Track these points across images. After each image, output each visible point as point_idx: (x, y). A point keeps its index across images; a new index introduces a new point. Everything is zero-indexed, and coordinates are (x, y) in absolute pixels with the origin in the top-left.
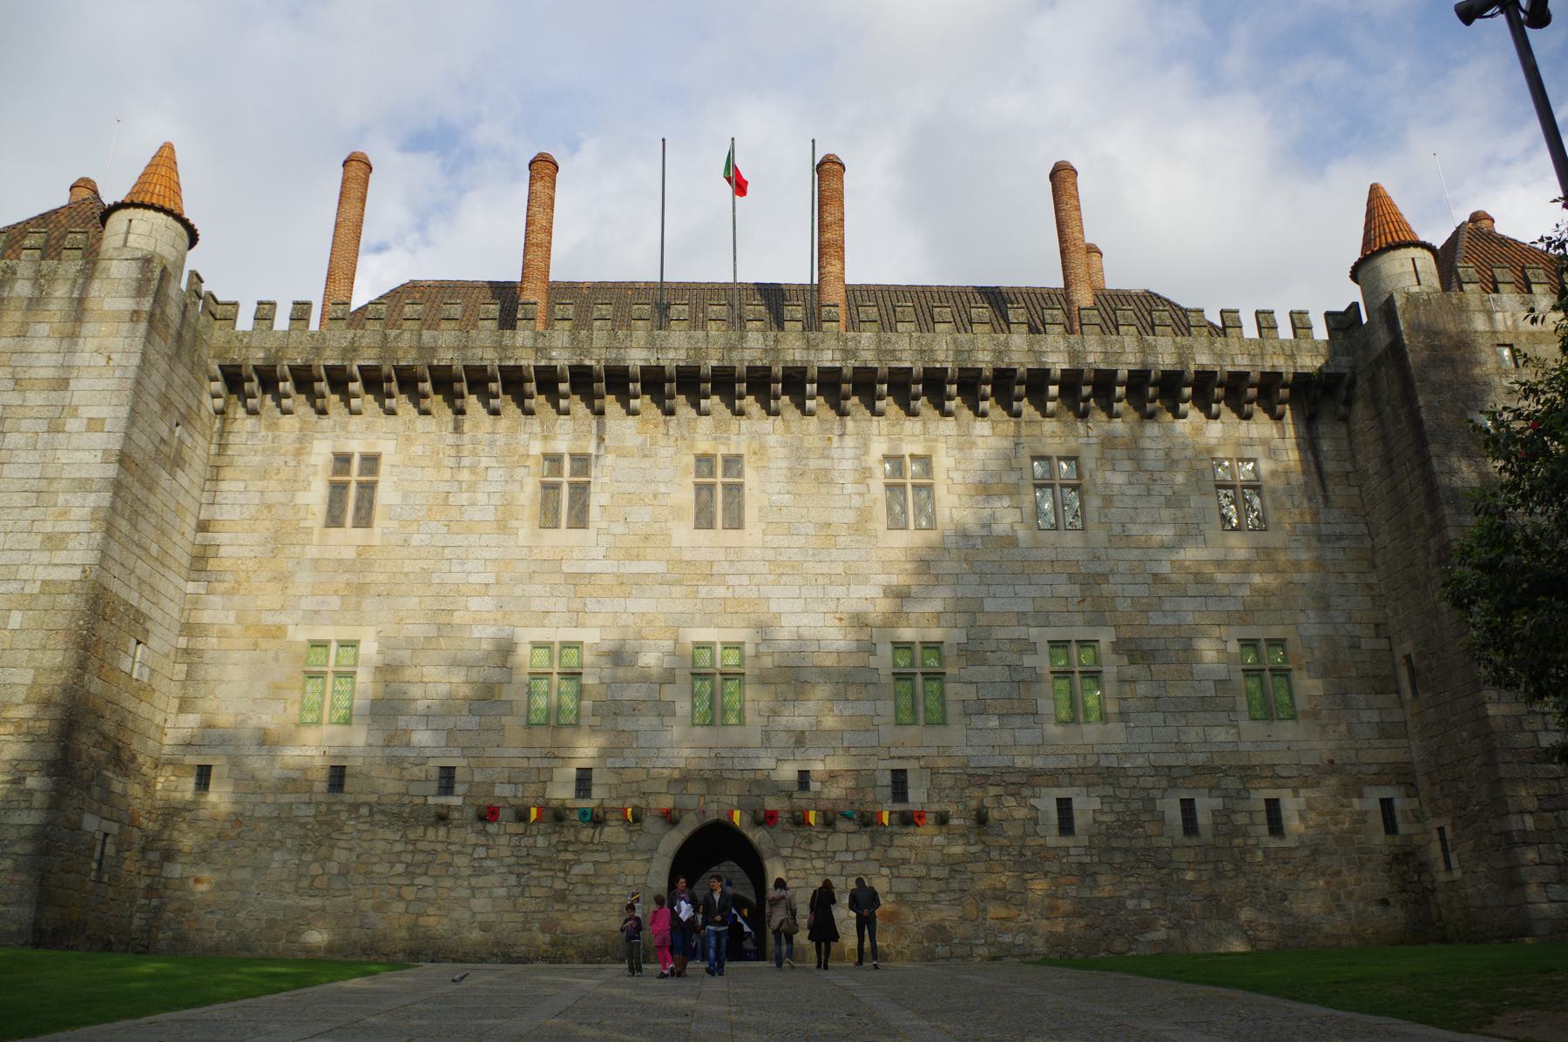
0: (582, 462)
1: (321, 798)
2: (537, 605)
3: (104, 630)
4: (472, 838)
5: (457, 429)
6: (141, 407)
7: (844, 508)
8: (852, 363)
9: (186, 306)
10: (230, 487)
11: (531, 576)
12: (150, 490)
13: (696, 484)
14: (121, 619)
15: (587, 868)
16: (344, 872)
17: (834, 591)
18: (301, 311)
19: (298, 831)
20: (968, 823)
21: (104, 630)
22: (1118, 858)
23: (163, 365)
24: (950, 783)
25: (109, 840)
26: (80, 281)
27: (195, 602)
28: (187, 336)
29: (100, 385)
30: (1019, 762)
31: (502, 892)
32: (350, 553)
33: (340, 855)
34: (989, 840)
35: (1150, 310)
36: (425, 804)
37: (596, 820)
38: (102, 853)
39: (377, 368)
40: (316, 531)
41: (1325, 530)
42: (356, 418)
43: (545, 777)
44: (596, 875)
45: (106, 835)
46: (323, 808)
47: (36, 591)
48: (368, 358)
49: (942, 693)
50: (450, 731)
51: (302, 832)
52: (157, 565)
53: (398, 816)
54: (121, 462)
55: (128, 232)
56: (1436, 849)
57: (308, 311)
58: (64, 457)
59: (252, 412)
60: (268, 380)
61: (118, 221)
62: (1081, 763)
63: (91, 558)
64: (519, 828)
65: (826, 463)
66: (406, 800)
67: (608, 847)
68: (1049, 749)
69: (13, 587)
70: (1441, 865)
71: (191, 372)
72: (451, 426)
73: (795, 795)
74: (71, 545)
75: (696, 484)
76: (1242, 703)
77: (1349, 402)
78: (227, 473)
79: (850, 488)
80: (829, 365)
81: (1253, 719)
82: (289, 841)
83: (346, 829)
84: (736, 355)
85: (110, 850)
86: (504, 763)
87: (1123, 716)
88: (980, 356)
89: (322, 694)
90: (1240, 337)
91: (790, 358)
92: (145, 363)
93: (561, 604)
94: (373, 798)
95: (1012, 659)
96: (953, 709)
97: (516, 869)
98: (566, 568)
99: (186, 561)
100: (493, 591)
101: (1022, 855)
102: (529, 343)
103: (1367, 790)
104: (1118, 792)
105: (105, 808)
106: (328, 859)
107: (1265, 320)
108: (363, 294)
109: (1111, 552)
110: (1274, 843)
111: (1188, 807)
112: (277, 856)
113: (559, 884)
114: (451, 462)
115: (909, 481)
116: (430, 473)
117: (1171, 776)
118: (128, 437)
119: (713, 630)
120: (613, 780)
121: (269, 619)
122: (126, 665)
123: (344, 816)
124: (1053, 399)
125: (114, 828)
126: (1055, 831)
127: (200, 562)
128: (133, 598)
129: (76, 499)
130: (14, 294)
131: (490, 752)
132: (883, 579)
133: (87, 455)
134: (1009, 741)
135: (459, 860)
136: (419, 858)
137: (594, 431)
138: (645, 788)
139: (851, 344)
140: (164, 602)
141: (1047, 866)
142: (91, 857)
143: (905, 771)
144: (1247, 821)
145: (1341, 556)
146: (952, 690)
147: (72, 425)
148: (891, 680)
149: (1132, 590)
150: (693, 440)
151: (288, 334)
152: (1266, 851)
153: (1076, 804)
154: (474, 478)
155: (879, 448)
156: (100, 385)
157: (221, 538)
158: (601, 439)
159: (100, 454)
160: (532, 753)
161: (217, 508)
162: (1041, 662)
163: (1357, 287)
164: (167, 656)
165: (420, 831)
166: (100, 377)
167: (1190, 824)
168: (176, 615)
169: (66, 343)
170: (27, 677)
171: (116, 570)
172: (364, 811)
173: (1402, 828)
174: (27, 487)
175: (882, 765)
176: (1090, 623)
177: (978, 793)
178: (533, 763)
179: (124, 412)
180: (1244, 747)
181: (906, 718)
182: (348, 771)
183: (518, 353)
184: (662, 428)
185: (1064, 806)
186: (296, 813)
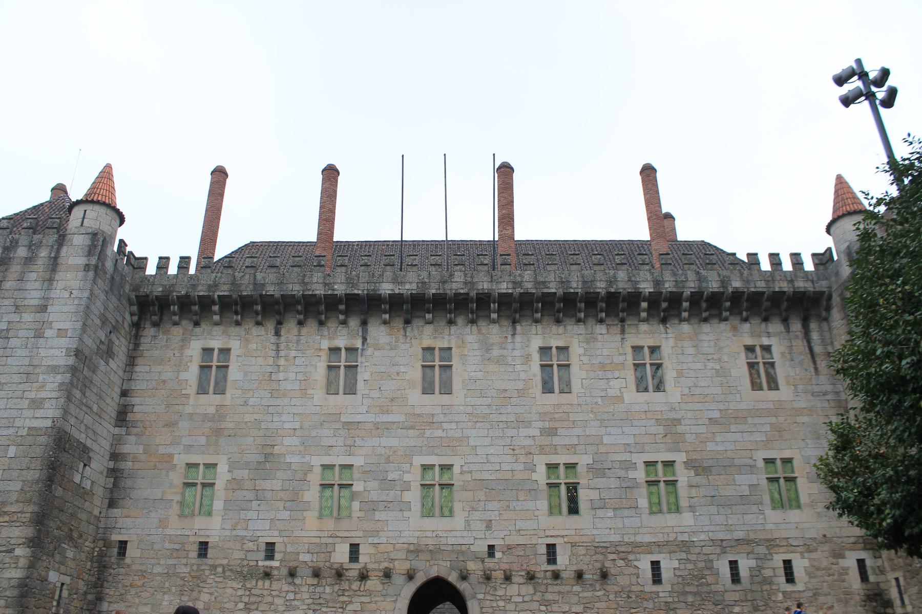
1: (193, 561)
2: (325, 442)
3: (64, 458)
4: (286, 587)
5: (277, 333)
6: (89, 322)
7: (515, 380)
8: (519, 290)
9: (117, 261)
11: (321, 424)
12: (94, 372)
13: (423, 366)
14: (75, 451)
17: (510, 432)
18: (184, 262)
21: (64, 458)
22: (690, 599)
23: (103, 296)
24: (583, 552)
25: (65, 587)
26: (56, 247)
27: (117, 440)
28: (117, 279)
29: (65, 309)
34: (608, 588)
35: (706, 254)
36: (257, 566)
38: (60, 596)
39: (229, 297)
40: (192, 397)
41: (816, 389)
42: (217, 328)
43: (328, 549)
45: (63, 584)
46: (195, 567)
47: (24, 434)
48: (224, 291)
51: (182, 582)
52: (97, 418)
53: (241, 572)
54: (75, 355)
55: (84, 218)
57: (188, 263)
58: (43, 352)
61: (77, 212)
62: (666, 538)
63: (58, 413)
64: (315, 581)
65: (505, 352)
66: (245, 563)
67: (370, 593)
68: (645, 530)
69: (11, 431)
71: (119, 300)
72: (273, 331)
73: (486, 560)
75: (423, 366)
76: (767, 499)
77: (828, 309)
78: (139, 361)
79: (519, 368)
80: (505, 291)
81: (774, 508)
82: (174, 588)
83: (209, 581)
84: (447, 286)
85: (65, 593)
87: (692, 508)
88: (598, 284)
89: (195, 496)
90: (759, 270)
91: (480, 287)
92: (92, 296)
93: (340, 442)
94: (225, 562)
95: (622, 473)
96: (583, 505)
97: (312, 606)
98: (343, 419)
99: (114, 415)
100: (298, 433)
101: (629, 597)
103: (847, 553)
104: (689, 556)
105: (62, 567)
106: (197, 599)
107: (775, 258)
108: (222, 250)
109: (683, 406)
110: (789, 588)
111: (734, 565)
114: (273, 354)
115: (555, 363)
116: (260, 361)
117: (722, 546)
118: (81, 340)
119: (434, 457)
120: (372, 550)
121: (162, 450)
122: (77, 479)
123: (207, 573)
124: (644, 311)
125: (67, 580)
126: (651, 582)
127: (123, 417)
128: (82, 438)
129: (50, 378)
131: (297, 533)
132: (540, 424)
133: (56, 352)
134: (621, 526)
135: (277, 601)
136: (253, 599)
137: (360, 334)
138: (392, 556)
139: (519, 279)
140: (101, 440)
141: (645, 604)
142: (53, 598)
143: (555, 545)
144: (772, 574)
145: (826, 405)
147: (48, 333)
148: (545, 487)
149: (695, 429)
150: (421, 339)
151: (176, 276)
152: (784, 593)
153: (663, 565)
155: (537, 342)
156: (65, 309)
157: (135, 400)
158: (364, 340)
159: (64, 351)
162: (640, 475)
163: (830, 238)
164: (101, 473)
165: (254, 582)
166: (66, 304)
167: (735, 577)
168: (108, 448)
169: (46, 283)
170: (19, 486)
171: (72, 421)
174: (21, 371)
175: (540, 541)
176: (669, 450)
177: (600, 557)
178: (324, 541)
179: (79, 325)
180: (769, 527)
181: (556, 511)
183: (314, 286)
184: (402, 332)
185: (655, 565)
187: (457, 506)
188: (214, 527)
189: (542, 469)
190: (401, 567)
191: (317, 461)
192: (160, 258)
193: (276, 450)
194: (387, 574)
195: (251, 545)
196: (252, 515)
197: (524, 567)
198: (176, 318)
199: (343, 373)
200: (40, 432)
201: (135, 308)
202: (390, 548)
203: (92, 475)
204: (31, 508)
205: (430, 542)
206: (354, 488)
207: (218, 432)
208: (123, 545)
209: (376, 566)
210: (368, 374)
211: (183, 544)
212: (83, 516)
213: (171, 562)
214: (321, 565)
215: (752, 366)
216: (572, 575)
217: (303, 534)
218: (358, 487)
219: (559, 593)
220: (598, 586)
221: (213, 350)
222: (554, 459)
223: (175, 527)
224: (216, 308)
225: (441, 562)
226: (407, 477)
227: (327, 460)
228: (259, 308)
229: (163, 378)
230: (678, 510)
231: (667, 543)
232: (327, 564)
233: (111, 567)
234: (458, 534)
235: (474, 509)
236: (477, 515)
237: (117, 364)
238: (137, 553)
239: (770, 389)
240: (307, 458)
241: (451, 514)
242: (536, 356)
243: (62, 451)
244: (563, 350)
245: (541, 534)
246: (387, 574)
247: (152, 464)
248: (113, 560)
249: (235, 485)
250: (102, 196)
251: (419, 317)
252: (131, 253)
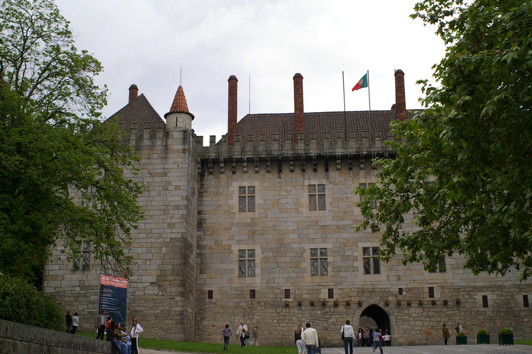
2: (311, 236)
4: (297, 311)
10: (207, 199)
15: (333, 320)
16: (258, 322)
19: (242, 310)
20: (454, 304)
24: (448, 291)
27: (199, 238)
29: (177, 174)
30: (470, 285)
32: (249, 221)
33: (256, 317)
34: (460, 309)
40: (237, 214)
42: (245, 174)
44: (337, 322)
46: (249, 303)
47: (168, 241)
48: (249, 155)
50: (287, 278)
59: (211, 173)
60: (216, 161)
68: (479, 280)
69: (161, 240)
74: (177, 227)
78: (205, 194)
86: (305, 288)
94: (265, 300)
96: (448, 267)
98: (320, 224)
101: (471, 314)
102: (303, 148)
106: (253, 318)
112: (237, 318)
113: (325, 325)
120: (340, 292)
121: (224, 243)
123: (256, 305)
126: (482, 306)
127: (200, 224)
130: (144, 144)
131: (300, 284)
135: (293, 318)
136: (281, 318)
141: (479, 317)
143: (433, 288)
147: (171, 188)
153: (488, 298)
154: (286, 194)
156: (177, 174)
157: (206, 216)
159: (180, 197)
160: (314, 284)
161: (203, 206)
166: (176, 172)
170: (170, 267)
172: (262, 303)
175: (425, 286)
178: (314, 288)
182: (256, 291)
185: (485, 298)
186: (241, 305)
188: (257, 282)
190: (355, 300)
191: (308, 247)
192: (211, 136)
193: (286, 241)
194: (348, 304)
195: (277, 291)
196: (276, 275)
197: (418, 299)
198: (222, 170)
199: (318, 200)
200: (176, 240)
201: (200, 165)
202: (349, 290)
203: (193, 259)
204: (180, 278)
205: (369, 287)
206: (329, 260)
207: (253, 233)
208: (210, 294)
209: (342, 300)
210: (331, 198)
211: (242, 291)
212: (193, 279)
213: (237, 300)
214: (314, 300)
216: (442, 302)
217: (304, 284)
218: (330, 259)
219: (436, 312)
220: (455, 309)
221: (245, 187)
223: (237, 283)
225: (375, 297)
226: (355, 254)
227: (313, 246)
228: (269, 163)
229: (221, 204)
231: (491, 287)
232: (317, 299)
233: (206, 304)
234: (383, 283)
235: (391, 270)
236: (392, 273)
237: (196, 198)
238: (219, 297)
240: (303, 245)
243: (184, 248)
245: (426, 282)
246: (348, 304)
247: (220, 251)
248: (207, 300)
249: (266, 260)
250: (179, 106)
251: (356, 166)
252: (195, 134)
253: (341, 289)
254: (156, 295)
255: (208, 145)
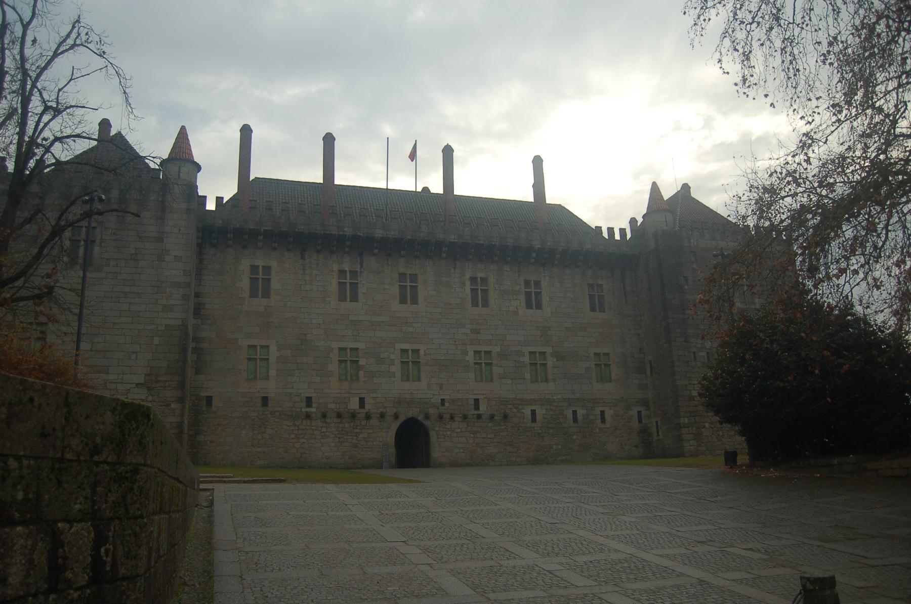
0: (354, 274)
5: (303, 258)
22: (551, 431)
31: (333, 444)
37: (368, 417)
49: (491, 370)
56: (654, 429)
70: (656, 434)
94: (280, 409)
107: (611, 230)
110: (602, 426)
111: (575, 412)
113: (354, 441)
127: (198, 311)
146: (495, 370)
155: (468, 275)
158: (362, 266)
162: (526, 359)
172: (277, 414)
173: (644, 421)
185: (533, 412)
187: (423, 375)
188: (272, 387)
189: (471, 353)
191: (335, 345)
194: (382, 416)
198: (230, 242)
201: (201, 234)
208: (209, 399)
215: (591, 297)
218: (362, 362)
221: (258, 267)
222: (478, 348)
224: (261, 238)
226: (392, 356)
227: (342, 345)
230: (547, 381)
239: (600, 311)
241: (419, 379)
242: (468, 283)
244: (484, 280)
248: (204, 408)
253: (374, 398)
254: (143, 400)
255: (214, 209)
